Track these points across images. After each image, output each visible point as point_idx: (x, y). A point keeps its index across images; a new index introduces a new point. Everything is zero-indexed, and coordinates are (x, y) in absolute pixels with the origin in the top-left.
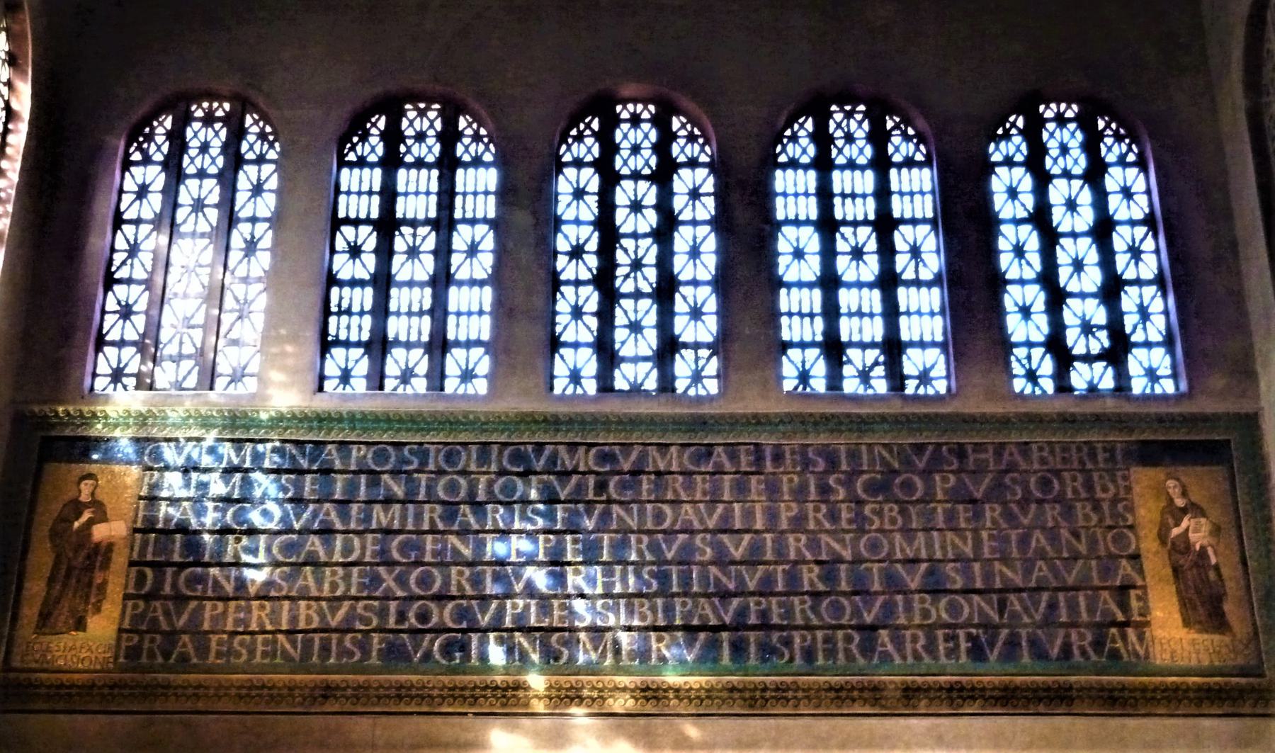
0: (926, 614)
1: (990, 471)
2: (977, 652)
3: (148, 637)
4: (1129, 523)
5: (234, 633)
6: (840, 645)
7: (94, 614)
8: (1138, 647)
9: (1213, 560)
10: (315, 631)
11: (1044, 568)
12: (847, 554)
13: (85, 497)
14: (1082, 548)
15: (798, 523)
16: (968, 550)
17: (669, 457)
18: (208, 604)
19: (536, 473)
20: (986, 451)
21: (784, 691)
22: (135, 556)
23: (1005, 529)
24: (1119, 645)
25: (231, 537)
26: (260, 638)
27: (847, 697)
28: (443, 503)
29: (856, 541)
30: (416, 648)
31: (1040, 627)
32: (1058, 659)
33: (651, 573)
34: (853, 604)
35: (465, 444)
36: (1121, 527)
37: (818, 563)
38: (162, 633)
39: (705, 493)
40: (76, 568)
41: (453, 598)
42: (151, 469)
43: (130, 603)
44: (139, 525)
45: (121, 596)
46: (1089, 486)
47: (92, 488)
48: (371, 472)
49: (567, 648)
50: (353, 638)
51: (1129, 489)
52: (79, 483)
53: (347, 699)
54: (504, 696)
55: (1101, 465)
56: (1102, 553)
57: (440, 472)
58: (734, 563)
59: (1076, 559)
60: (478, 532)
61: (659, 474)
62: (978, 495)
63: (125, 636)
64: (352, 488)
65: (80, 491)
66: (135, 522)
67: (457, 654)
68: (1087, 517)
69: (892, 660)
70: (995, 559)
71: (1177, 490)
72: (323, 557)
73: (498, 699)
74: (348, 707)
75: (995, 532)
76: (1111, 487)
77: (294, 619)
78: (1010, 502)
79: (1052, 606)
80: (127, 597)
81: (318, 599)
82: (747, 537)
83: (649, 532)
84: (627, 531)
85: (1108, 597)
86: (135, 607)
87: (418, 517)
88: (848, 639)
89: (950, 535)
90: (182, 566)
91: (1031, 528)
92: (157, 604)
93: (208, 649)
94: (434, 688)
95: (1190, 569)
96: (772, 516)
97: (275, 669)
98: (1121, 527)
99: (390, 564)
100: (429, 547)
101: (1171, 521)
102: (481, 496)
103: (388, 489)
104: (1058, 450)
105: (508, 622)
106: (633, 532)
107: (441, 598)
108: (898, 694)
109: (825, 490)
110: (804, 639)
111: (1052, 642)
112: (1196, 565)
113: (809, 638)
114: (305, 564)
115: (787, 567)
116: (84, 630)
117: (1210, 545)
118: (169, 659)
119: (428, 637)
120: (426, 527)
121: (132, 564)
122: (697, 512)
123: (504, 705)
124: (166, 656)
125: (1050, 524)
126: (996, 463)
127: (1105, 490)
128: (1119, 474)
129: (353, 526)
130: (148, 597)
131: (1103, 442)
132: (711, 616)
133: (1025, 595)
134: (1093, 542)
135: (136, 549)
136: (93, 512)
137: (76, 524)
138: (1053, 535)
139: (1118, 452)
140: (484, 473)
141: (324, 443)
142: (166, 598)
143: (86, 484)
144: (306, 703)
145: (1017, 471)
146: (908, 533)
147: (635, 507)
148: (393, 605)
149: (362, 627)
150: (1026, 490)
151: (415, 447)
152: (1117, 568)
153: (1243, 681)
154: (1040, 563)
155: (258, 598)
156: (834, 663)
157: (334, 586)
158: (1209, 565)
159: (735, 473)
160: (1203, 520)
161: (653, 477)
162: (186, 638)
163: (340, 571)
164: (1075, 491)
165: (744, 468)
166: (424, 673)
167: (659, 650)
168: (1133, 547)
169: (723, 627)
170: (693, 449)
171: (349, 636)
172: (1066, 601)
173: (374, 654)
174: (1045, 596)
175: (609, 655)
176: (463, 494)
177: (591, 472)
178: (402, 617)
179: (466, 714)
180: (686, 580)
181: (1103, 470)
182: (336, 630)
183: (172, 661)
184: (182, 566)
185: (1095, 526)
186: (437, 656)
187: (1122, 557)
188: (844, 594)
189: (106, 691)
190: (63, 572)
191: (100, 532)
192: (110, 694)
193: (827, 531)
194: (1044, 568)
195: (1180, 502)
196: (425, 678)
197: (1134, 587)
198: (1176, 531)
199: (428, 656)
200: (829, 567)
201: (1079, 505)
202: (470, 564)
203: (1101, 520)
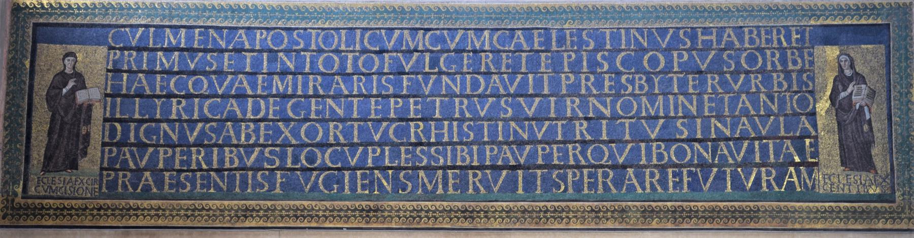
0: (660, 157)
1: (714, 50)
2: (694, 186)
3: (121, 173)
4: (811, 88)
5: (180, 171)
6: (600, 179)
7: (82, 157)
8: (808, 181)
9: (868, 117)
10: (236, 169)
11: (746, 122)
12: (607, 112)
13: (68, 71)
14: (775, 108)
15: (574, 90)
16: (694, 110)
17: (483, 39)
18: (161, 150)
19: (387, 51)
20: (711, 34)
21: (560, 212)
22: (108, 115)
23: (721, 93)
24: (795, 179)
25: (174, 100)
26: (199, 174)
27: (604, 217)
28: (322, 74)
29: (613, 103)
30: (307, 181)
31: (739, 166)
32: (750, 189)
33: (469, 127)
34: (611, 149)
35: (337, 29)
36: (803, 92)
37: (586, 119)
38: (131, 171)
39: (508, 67)
40: (67, 123)
41: (331, 145)
42: (114, 48)
43: (107, 149)
44: (108, 91)
45: (100, 143)
46: (784, 61)
47: (73, 63)
48: (270, 51)
49: (410, 182)
50: (262, 174)
51: (812, 63)
52: (63, 59)
53: (261, 218)
54: (368, 216)
55: (794, 45)
56: (789, 111)
57: (320, 51)
58: (528, 119)
59: (769, 116)
60: (347, 96)
61: (475, 51)
62: (703, 67)
63: (105, 173)
64: (257, 63)
65: (65, 66)
66: (106, 89)
67: (335, 186)
68: (780, 85)
69: (636, 190)
70: (712, 116)
71: (847, 63)
72: (239, 115)
73: (363, 218)
74: (261, 223)
75: (713, 96)
76: (799, 61)
77: (221, 161)
78: (726, 72)
79: (750, 150)
80: (104, 144)
81: (237, 146)
82: (537, 100)
83: (468, 97)
84: (451, 95)
85: (789, 144)
86: (110, 152)
87: (305, 85)
88: (606, 175)
89: (681, 98)
90: (141, 121)
91: (740, 92)
92: (126, 149)
93: (163, 182)
94: (320, 210)
95: (851, 123)
96: (555, 83)
97: (210, 197)
98: (803, 92)
99: (287, 120)
100: (313, 108)
101: (840, 87)
102: (349, 70)
103: (283, 63)
104: (763, 32)
105: (370, 163)
106: (457, 96)
107: (323, 145)
108: (639, 215)
109: (594, 65)
110: (574, 175)
111: (747, 179)
112: (855, 120)
113: (578, 175)
114: (227, 120)
115: (564, 122)
116: (77, 169)
117: (867, 105)
118: (137, 189)
119: (315, 173)
120: (311, 92)
121: (106, 120)
122: (502, 81)
123: (367, 223)
124: (135, 187)
125: (754, 90)
126: (717, 44)
127: (795, 63)
128: (806, 51)
129: (259, 92)
130: (119, 145)
131: (797, 26)
132: (511, 158)
133: (731, 143)
134: (782, 102)
135: (108, 109)
137: (64, 91)
138: (754, 98)
139: (807, 35)
140: (351, 51)
141: (236, 28)
142: (132, 145)
143: (69, 60)
144: (232, 221)
145: (732, 49)
146: (652, 97)
147: (458, 77)
148: (290, 150)
149: (269, 167)
150: (738, 63)
151: (302, 31)
152: (798, 123)
153: (878, 205)
154: (744, 119)
155: (194, 145)
156: (595, 192)
157: (248, 137)
158: (865, 120)
159: (529, 51)
160: (863, 86)
161: (471, 54)
162: (147, 174)
163: (252, 125)
164: (773, 63)
165: (536, 47)
166: (313, 200)
167: (474, 183)
168: (811, 107)
169: (518, 167)
170: (499, 32)
171: (260, 173)
172: (760, 148)
173: (278, 185)
174: (746, 144)
175: (440, 186)
176: (336, 67)
177: (428, 51)
178: (296, 160)
179: (341, 228)
180: (493, 132)
181: (795, 48)
182: (251, 169)
183: (139, 190)
184: (141, 121)
185: (785, 91)
186: (322, 188)
187: (802, 114)
188: (603, 142)
189: (95, 212)
190: (58, 127)
191: (81, 96)
192: (98, 214)
193: (594, 96)
194: (746, 122)
195: (848, 72)
196: (314, 203)
197: (809, 137)
198: (843, 95)
199: (315, 187)
200: (593, 121)
201: (775, 75)
202: (341, 120)
203: (790, 86)
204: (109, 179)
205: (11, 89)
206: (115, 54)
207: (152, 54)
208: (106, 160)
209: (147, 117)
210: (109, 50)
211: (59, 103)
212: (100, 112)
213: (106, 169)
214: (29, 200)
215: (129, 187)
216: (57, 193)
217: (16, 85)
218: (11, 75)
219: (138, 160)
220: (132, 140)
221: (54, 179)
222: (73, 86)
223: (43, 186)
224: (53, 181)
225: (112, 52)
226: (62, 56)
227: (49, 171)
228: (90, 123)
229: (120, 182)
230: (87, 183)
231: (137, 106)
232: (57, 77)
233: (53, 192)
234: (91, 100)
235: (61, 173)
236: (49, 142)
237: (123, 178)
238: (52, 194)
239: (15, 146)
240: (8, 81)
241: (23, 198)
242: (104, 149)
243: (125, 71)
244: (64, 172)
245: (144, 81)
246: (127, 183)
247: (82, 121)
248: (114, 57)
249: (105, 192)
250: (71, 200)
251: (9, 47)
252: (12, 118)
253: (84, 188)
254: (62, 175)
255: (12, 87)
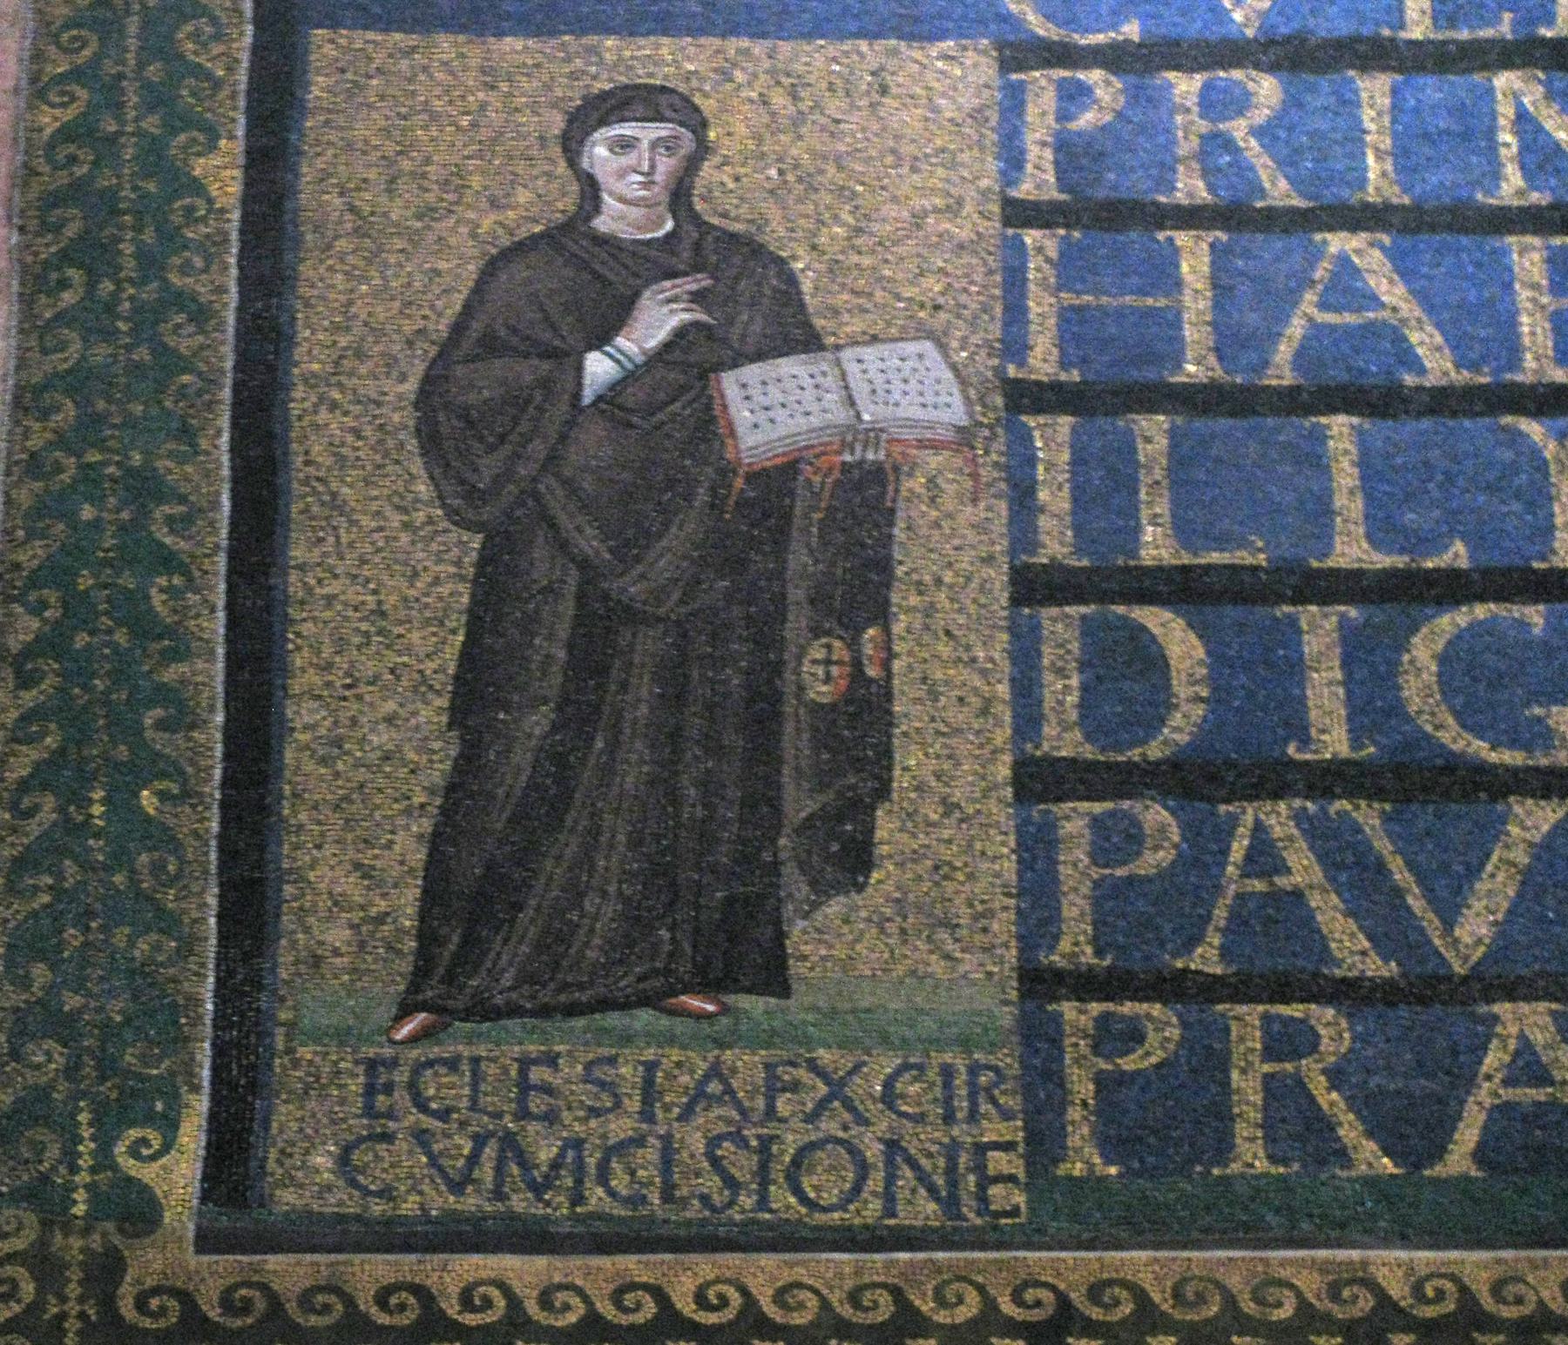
7: (823, 890)
40: (632, 615)
44: (1043, 361)
45: (1003, 771)
47: (666, 165)
52: (572, 143)
65: (591, 189)
66: (1014, 346)
92: (1279, 817)
116: (775, 980)
118: (1438, 1152)
135: (1054, 496)
136: (698, 297)
137: (598, 368)
143: (624, 145)
183: (1459, 1159)
204: (1128, 1064)
205: (62, 362)
206: (1074, 96)
207: (1431, 89)
208: (1075, 909)
209: (1457, 554)
210: (1005, 66)
211: (552, 460)
212: (980, 527)
213: (1085, 985)
214: (274, 1261)
215: (1349, 1130)
216: (578, 1199)
217: (109, 335)
218: (65, 257)
219: (1416, 903)
220: (1335, 742)
221: (537, 1074)
222: (680, 333)
223: (421, 1137)
224: (525, 1087)
225: (1042, 85)
226: (557, 123)
227: (484, 1011)
228: (882, 615)
229: (1247, 1087)
230: (889, 1097)
231: (1345, 476)
232: (520, 271)
233: (537, 1189)
234: (873, 435)
235: (613, 1019)
236: (468, 764)
237: (1269, 1054)
238: (520, 1202)
239: (122, 802)
240: (26, 302)
241: (207, 1242)
242: (1049, 827)
243: (1191, 217)
244: (644, 1017)
245: (1392, 292)
246: (1329, 1099)
247: (796, 594)
248: (1063, 116)
249: (1094, 1182)
250: (733, 1259)
251: (38, 56)
252: (85, 581)
253: (873, 1151)
254: (627, 1039)
255: (75, 347)
